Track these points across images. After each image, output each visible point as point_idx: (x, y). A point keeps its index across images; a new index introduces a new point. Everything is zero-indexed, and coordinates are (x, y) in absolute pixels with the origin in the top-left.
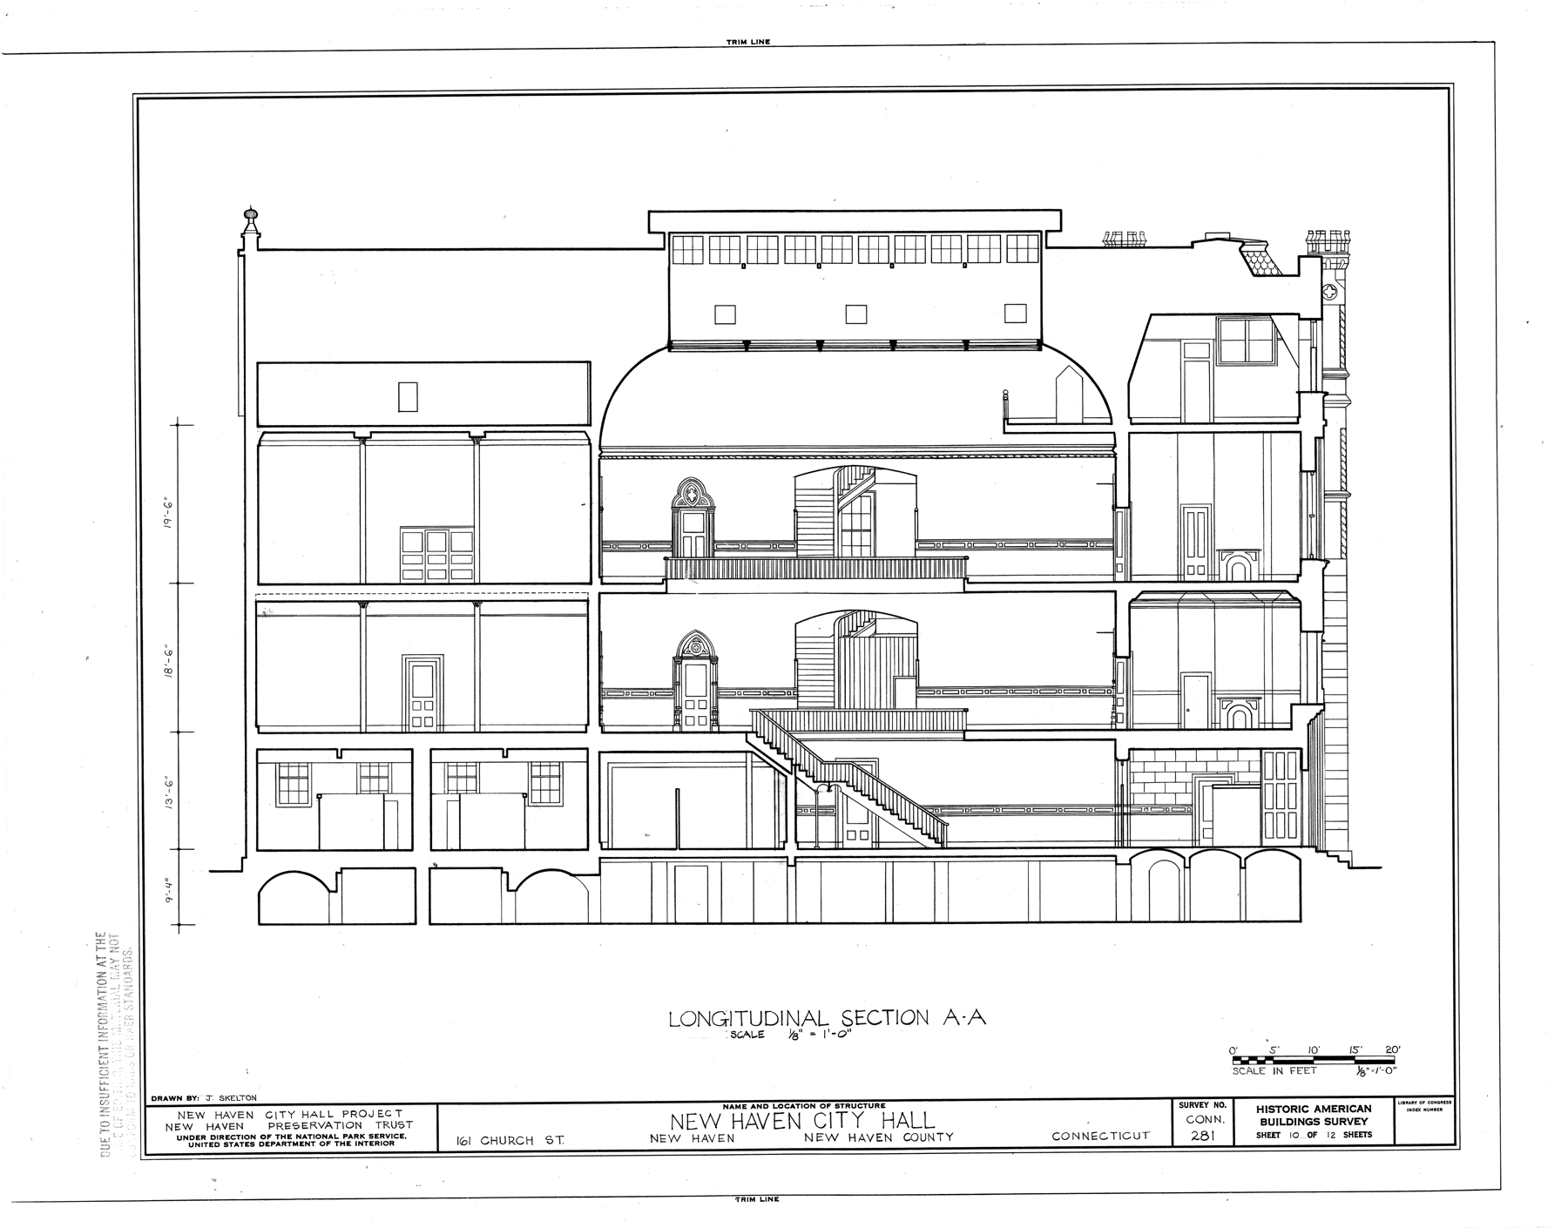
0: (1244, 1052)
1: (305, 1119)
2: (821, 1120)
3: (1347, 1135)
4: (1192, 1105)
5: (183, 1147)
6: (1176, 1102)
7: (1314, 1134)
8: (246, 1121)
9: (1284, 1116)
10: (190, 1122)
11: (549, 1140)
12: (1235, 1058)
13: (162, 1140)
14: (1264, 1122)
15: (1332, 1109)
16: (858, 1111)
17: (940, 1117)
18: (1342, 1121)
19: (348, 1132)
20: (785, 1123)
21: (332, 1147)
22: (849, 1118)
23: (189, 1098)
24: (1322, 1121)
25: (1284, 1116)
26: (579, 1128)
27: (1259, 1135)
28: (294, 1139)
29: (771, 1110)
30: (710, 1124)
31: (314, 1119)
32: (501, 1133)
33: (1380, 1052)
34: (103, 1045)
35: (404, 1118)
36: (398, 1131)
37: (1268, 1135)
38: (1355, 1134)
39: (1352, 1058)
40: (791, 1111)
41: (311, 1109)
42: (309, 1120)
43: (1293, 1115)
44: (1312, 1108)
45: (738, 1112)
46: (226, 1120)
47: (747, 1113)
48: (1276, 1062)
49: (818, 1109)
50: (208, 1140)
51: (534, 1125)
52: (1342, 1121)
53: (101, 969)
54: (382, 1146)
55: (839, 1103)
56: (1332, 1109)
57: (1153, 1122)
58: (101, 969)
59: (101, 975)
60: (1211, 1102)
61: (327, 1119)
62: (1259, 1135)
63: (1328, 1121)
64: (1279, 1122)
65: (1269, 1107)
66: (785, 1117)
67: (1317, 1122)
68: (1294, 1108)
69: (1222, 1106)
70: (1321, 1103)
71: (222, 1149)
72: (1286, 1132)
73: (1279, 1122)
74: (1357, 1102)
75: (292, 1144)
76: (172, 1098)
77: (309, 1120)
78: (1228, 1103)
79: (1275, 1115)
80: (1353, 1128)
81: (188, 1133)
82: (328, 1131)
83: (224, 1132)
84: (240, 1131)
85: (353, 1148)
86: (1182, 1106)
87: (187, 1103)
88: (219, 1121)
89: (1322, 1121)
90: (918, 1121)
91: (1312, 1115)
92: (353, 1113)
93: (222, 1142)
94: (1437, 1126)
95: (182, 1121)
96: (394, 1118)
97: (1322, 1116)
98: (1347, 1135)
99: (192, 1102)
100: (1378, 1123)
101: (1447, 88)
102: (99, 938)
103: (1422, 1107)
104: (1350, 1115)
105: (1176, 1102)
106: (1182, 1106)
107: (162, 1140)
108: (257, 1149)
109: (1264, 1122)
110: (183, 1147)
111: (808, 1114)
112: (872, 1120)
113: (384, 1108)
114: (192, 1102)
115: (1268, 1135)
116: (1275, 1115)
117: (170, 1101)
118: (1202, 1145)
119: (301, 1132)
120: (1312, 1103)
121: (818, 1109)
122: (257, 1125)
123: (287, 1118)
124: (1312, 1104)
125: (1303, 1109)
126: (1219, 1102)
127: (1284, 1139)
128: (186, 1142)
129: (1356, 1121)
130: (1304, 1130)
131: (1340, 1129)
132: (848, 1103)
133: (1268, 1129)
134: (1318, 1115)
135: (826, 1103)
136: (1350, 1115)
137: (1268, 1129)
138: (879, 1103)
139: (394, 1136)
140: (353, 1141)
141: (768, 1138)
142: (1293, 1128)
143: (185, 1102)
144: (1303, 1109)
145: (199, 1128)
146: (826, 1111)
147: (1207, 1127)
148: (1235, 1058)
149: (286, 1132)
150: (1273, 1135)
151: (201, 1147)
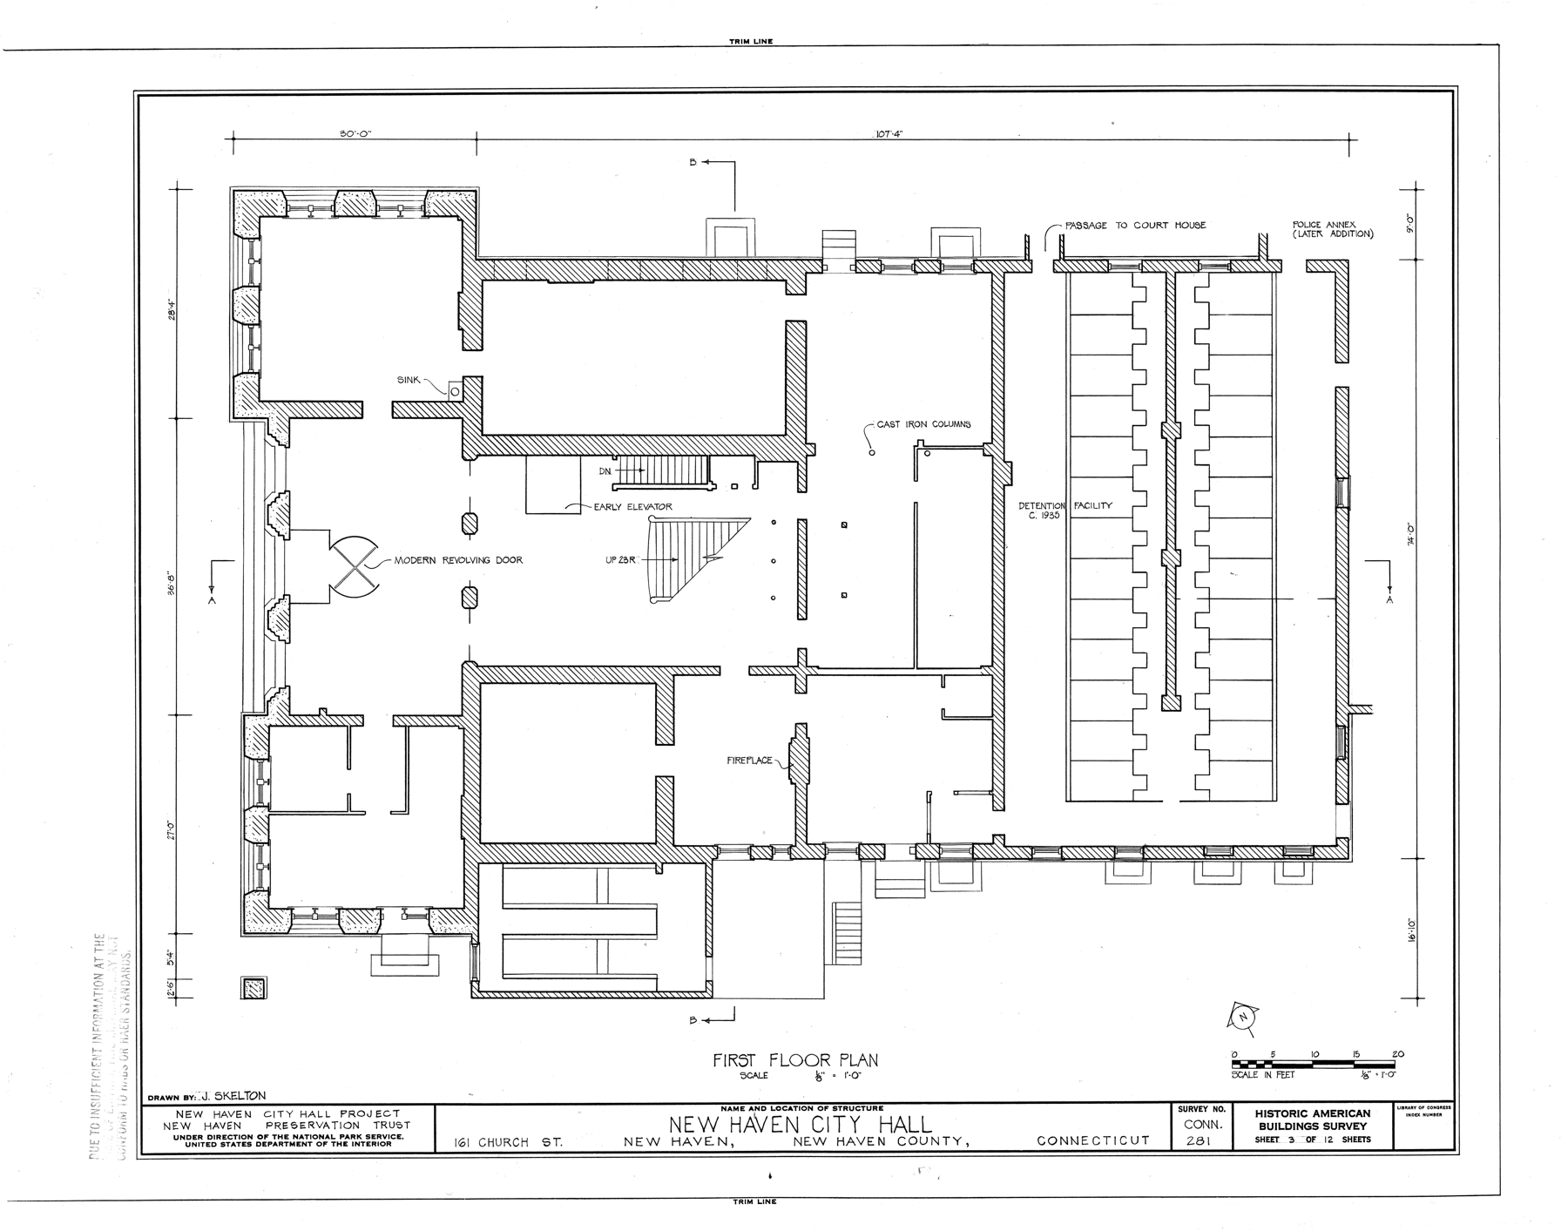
0: (1244, 1057)
1: (304, 1119)
2: (819, 1124)
3: (1346, 1140)
4: (1191, 1109)
5: (180, 1146)
6: (1176, 1106)
7: (1313, 1138)
8: (243, 1120)
9: (1282, 1121)
10: (188, 1121)
11: (546, 1142)
12: (1235, 1062)
13: (158, 1139)
14: (1263, 1126)
15: (1331, 1113)
16: (855, 1114)
17: (941, 1122)
18: (1341, 1126)
19: (345, 1132)
20: (782, 1127)
21: (329, 1148)
22: (847, 1123)
23: (186, 1098)
24: (1321, 1126)
25: (1282, 1121)
26: (576, 1129)
27: (1258, 1140)
28: (291, 1139)
29: (769, 1113)
30: (708, 1128)
31: (312, 1118)
32: (499, 1136)
33: (1385, 1056)
34: (96, 1046)
35: (402, 1118)
36: (396, 1131)
37: (1266, 1139)
38: (1354, 1139)
39: (1351, 1062)
40: (789, 1113)
41: (309, 1109)
42: (306, 1120)
43: (1292, 1120)
44: (1311, 1113)
45: (736, 1115)
46: (225, 1120)
47: (746, 1114)
48: (1275, 1066)
49: (816, 1112)
50: (205, 1140)
51: (532, 1127)
52: (1341, 1126)
53: (98, 971)
54: (379, 1146)
55: (837, 1105)
56: (1331, 1113)
57: (1153, 1125)
58: (98, 971)
59: (98, 976)
60: (1211, 1106)
61: (324, 1120)
62: (1258, 1140)
63: (1327, 1126)
64: (1277, 1126)
65: (1268, 1112)
66: (782, 1122)
67: (1316, 1126)
68: (1293, 1113)
69: (1221, 1110)
70: (1320, 1107)
71: (218, 1149)
72: (1284, 1135)
73: (1277, 1126)
74: (1357, 1107)
75: (290, 1146)
76: (169, 1098)
77: (306, 1120)
78: (1228, 1107)
79: (1274, 1120)
80: (1352, 1133)
81: (185, 1132)
82: (325, 1132)
83: (225, 1132)
84: (238, 1132)
85: (350, 1148)
86: (1181, 1110)
87: (185, 1104)
88: (218, 1120)
89: (1321, 1126)
90: (916, 1126)
91: (1311, 1119)
92: (352, 1114)
93: (219, 1142)
94: (1436, 1131)
95: (180, 1120)
96: (393, 1119)
97: (1321, 1121)
98: (1346, 1140)
99: (189, 1102)
100: (1377, 1127)
101: (1451, 91)
102: (99, 941)
103: (1421, 1112)
104: (1349, 1120)
105: (1176, 1106)
106: (1181, 1110)
107: (158, 1139)
108: (254, 1149)
109: (1263, 1126)
110: (180, 1146)
111: (805, 1117)
112: (869, 1120)
113: (383, 1108)
114: (189, 1102)
115: (1266, 1139)
116: (1274, 1120)
117: (168, 1101)
118: (1199, 1150)
119: (299, 1132)
120: (1307, 1108)
121: (816, 1112)
122: (255, 1123)
123: (285, 1118)
124: (1311, 1108)
125: (1302, 1114)
126: (1218, 1106)
127: (1284, 1143)
128: (183, 1142)
129: (1355, 1125)
130: (1300, 1135)
131: (1338, 1135)
132: (845, 1105)
133: (1266, 1133)
134: (1317, 1119)
135: (823, 1105)
136: (1349, 1120)
137: (1266, 1133)
138: (877, 1106)
139: (391, 1137)
140: (350, 1142)
141: (766, 1140)
142: (1291, 1133)
143: (181, 1101)
144: (1302, 1114)
145: (197, 1127)
146: (823, 1114)
147: (1205, 1132)
148: (1235, 1062)
149: (283, 1132)
150: (1272, 1139)
151: (197, 1147)
